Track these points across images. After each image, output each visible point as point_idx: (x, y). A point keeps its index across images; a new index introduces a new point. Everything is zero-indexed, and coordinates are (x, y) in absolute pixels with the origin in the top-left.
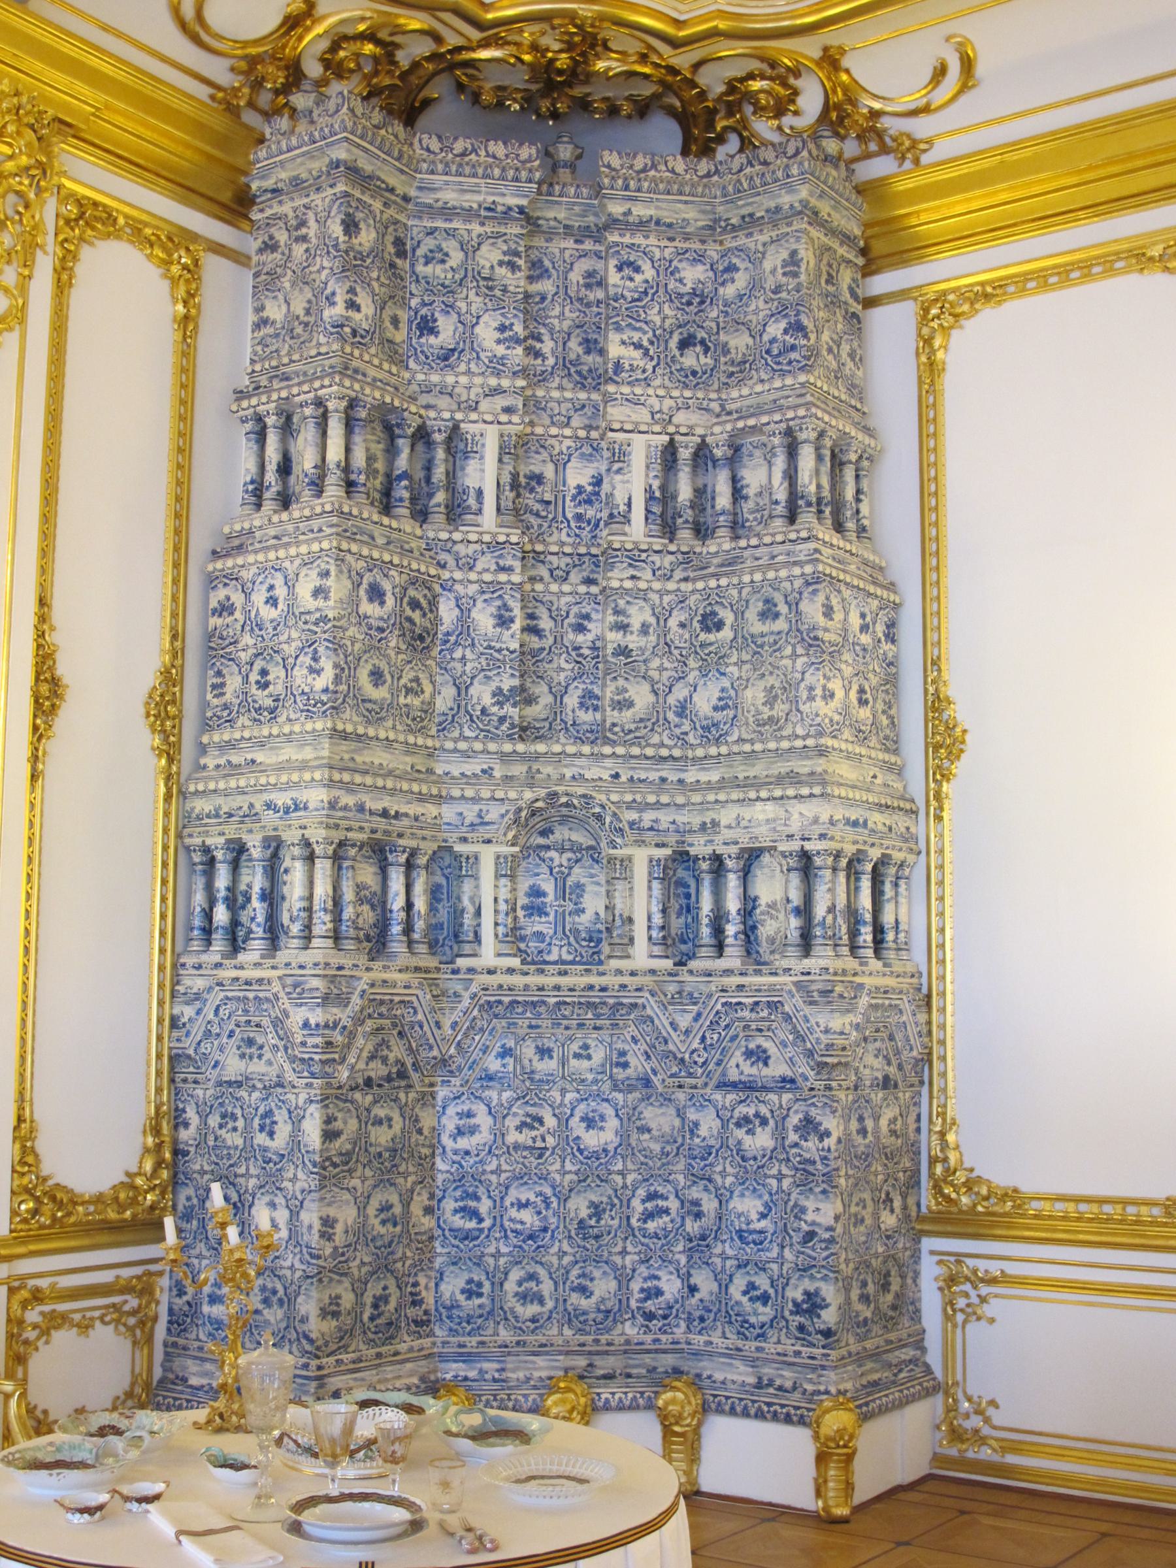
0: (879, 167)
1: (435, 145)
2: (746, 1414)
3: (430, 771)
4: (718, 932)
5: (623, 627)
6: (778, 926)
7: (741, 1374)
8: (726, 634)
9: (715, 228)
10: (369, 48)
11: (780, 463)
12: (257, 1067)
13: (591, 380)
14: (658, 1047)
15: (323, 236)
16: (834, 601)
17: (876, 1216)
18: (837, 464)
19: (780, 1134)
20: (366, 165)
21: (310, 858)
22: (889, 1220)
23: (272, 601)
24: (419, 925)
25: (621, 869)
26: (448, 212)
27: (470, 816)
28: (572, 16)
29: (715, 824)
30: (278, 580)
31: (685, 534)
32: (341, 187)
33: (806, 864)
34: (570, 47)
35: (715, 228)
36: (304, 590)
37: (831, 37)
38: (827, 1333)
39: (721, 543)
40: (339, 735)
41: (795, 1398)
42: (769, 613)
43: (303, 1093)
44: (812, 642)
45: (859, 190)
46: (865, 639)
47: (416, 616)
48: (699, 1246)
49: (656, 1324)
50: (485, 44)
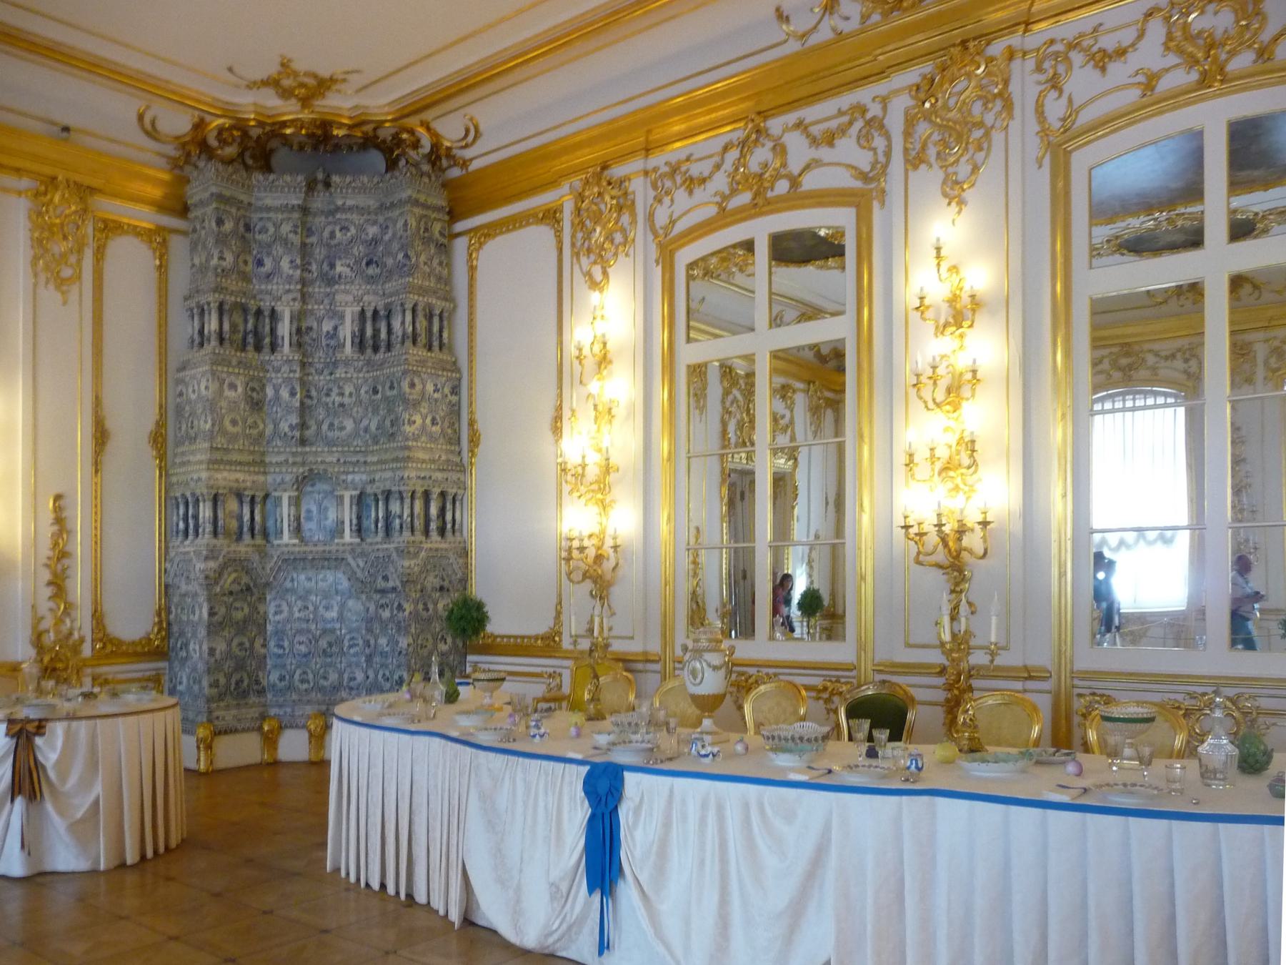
3: (262, 461)
8: (379, 396)
9: (382, 208)
16: (416, 381)
19: (392, 610)
24: (257, 527)
25: (340, 499)
31: (369, 351)
33: (402, 499)
35: (382, 208)
39: (380, 356)
42: (392, 387)
44: (405, 401)
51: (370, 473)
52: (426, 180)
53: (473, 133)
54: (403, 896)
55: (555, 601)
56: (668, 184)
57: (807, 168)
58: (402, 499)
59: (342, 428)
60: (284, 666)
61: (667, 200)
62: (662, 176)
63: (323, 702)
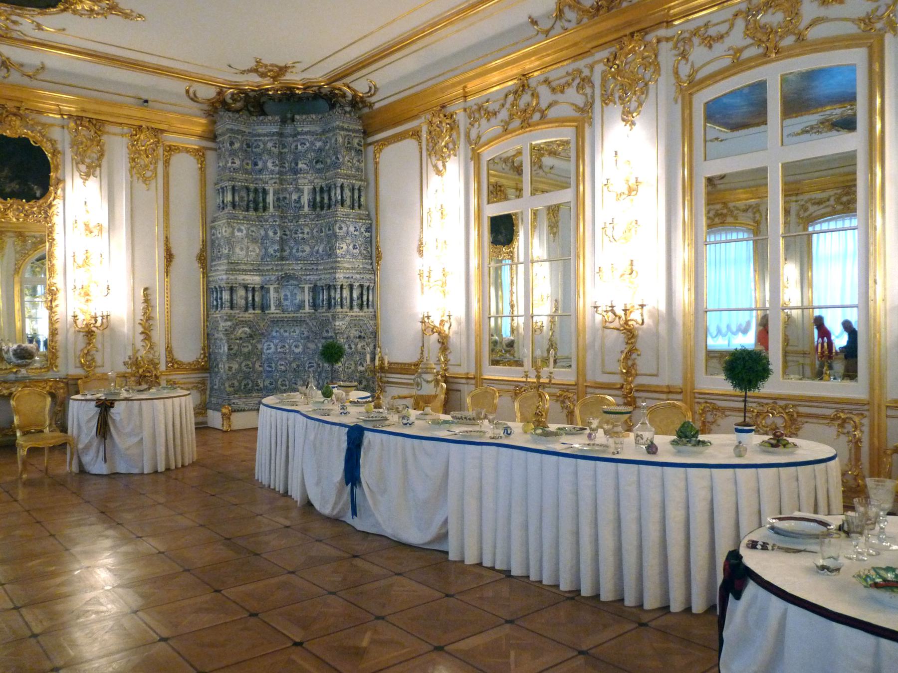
5: (303, 233)
9: (324, 132)
13: (296, 172)
14: (310, 330)
16: (343, 225)
22: (361, 368)
31: (318, 209)
35: (324, 132)
39: (324, 212)
42: (329, 230)
44: (336, 236)
48: (320, 374)
51: (319, 275)
52: (348, 116)
53: (373, 90)
56: (477, 116)
57: (550, 106)
58: (335, 289)
60: (272, 377)
61: (476, 124)
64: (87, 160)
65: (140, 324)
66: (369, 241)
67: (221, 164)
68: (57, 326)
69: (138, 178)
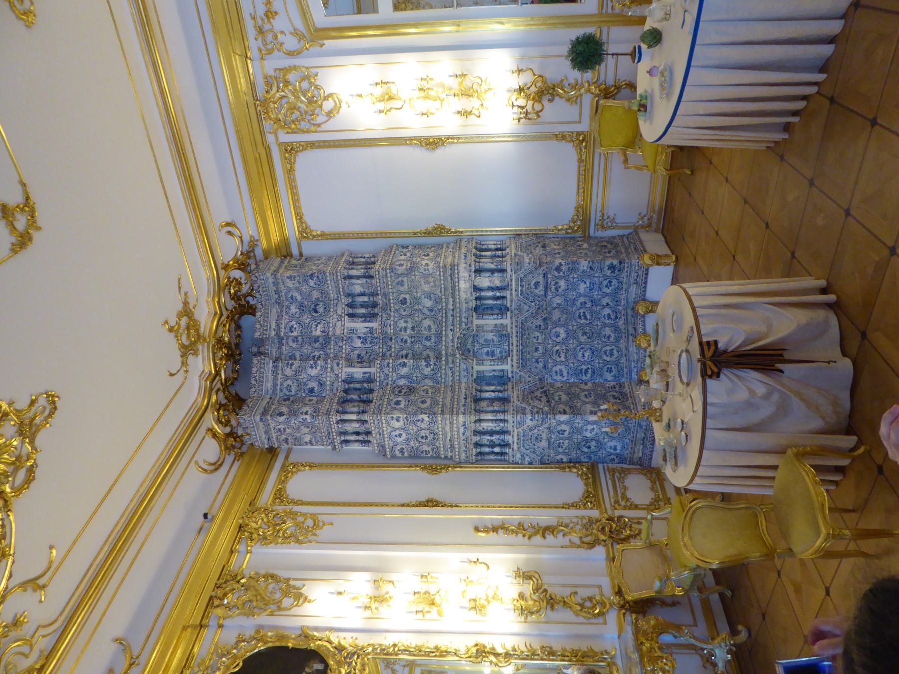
0: (259, 253)
1: (253, 390)
2: (645, 287)
4: (498, 298)
5: (405, 328)
6: (497, 281)
7: (633, 289)
8: (407, 296)
9: (278, 303)
10: (221, 412)
11: (354, 281)
12: (544, 436)
13: (327, 339)
14: (535, 316)
15: (283, 423)
17: (584, 249)
18: (353, 263)
19: (560, 278)
20: (261, 410)
21: (480, 421)
23: (400, 435)
24: (499, 388)
26: (275, 385)
27: (465, 374)
28: (214, 346)
29: (466, 299)
30: (394, 434)
31: (376, 310)
32: (269, 418)
33: (479, 271)
34: (221, 349)
36: (397, 425)
37: (219, 266)
38: (620, 263)
39: (379, 299)
40: (442, 413)
41: (640, 272)
43: (552, 421)
44: (411, 270)
45: (266, 258)
46: (408, 254)
47: (403, 391)
49: (618, 315)
50: (220, 376)
54: (821, 77)
55: (554, 143)
59: (429, 328)
62: (264, 40)
63: (627, 338)
64: (278, 595)
65: (530, 538)
66: (420, 246)
67: (307, 439)
68: (537, 646)
69: (315, 535)
